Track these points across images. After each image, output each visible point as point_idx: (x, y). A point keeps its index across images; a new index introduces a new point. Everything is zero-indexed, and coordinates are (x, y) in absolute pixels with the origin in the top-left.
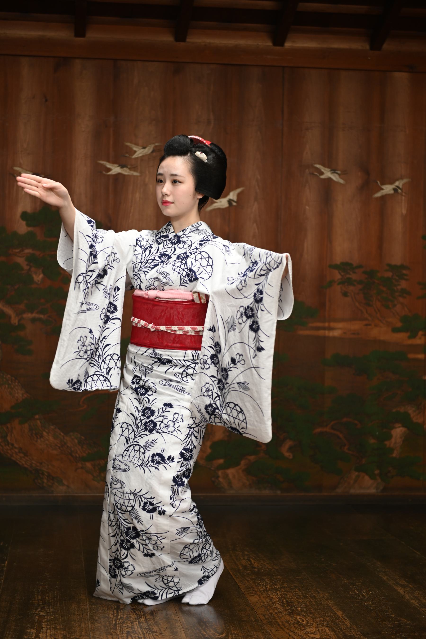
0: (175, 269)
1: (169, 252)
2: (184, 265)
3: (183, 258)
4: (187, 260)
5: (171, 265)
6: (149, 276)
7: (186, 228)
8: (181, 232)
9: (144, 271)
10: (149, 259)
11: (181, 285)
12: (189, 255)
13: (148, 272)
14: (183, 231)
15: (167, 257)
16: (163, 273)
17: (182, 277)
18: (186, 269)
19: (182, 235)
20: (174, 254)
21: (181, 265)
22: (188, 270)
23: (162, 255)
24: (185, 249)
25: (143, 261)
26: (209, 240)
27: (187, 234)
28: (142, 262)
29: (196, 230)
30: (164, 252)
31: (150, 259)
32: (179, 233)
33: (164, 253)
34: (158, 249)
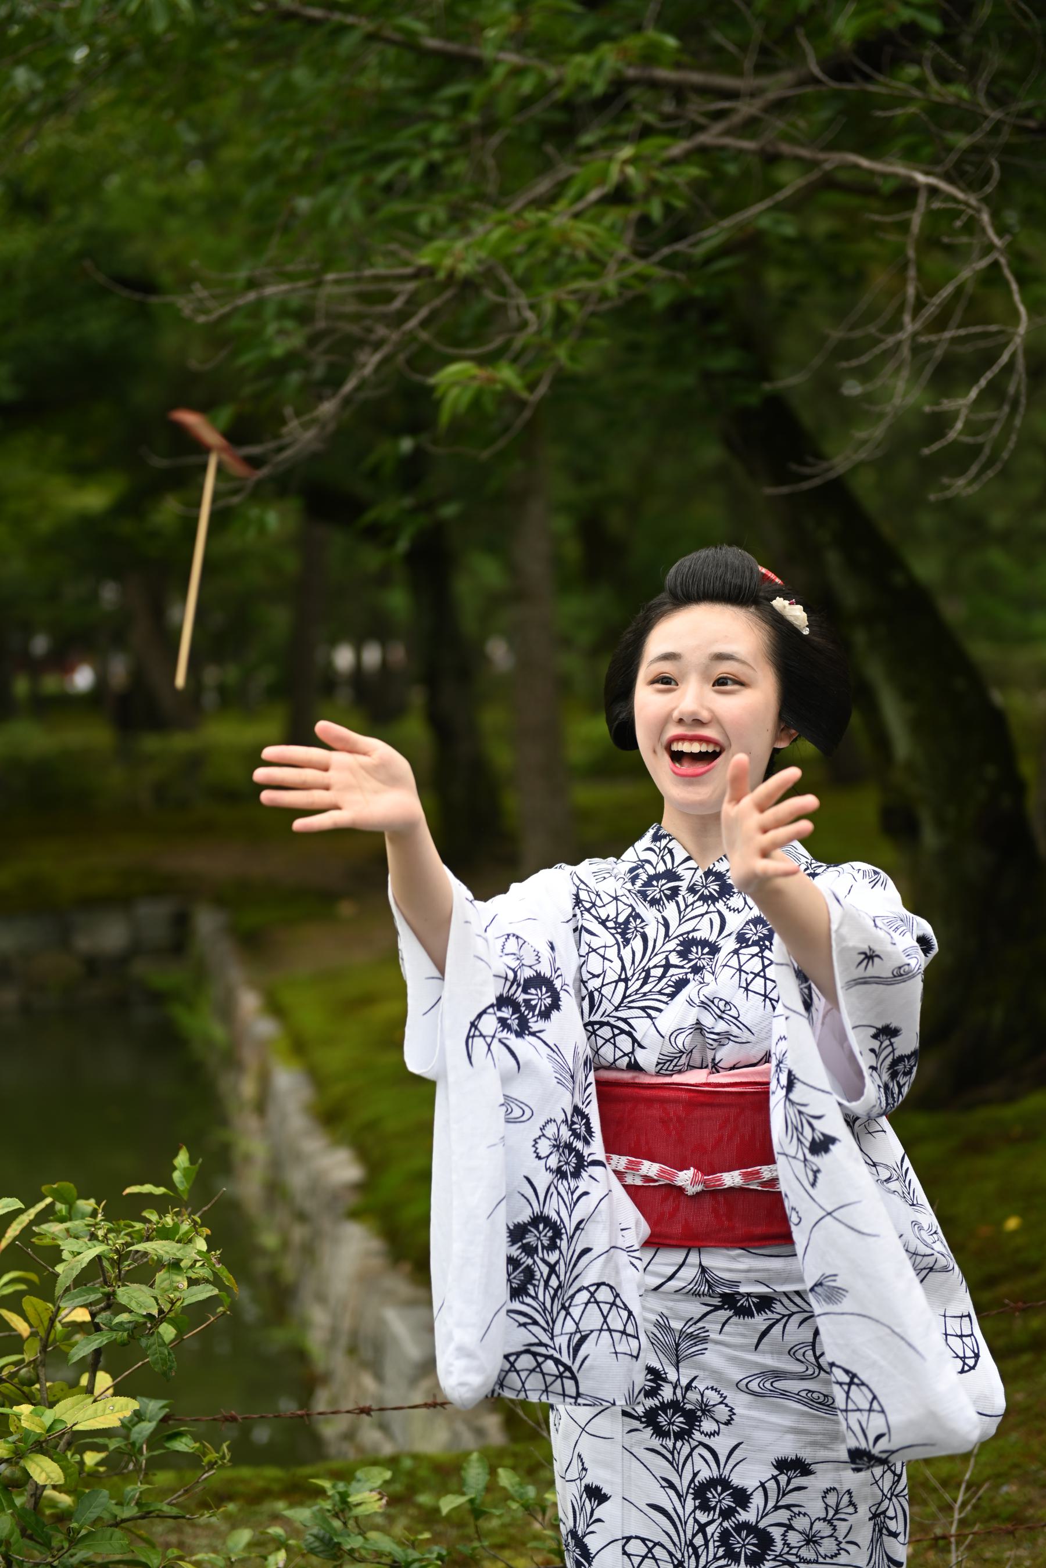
13: (660, 1010)
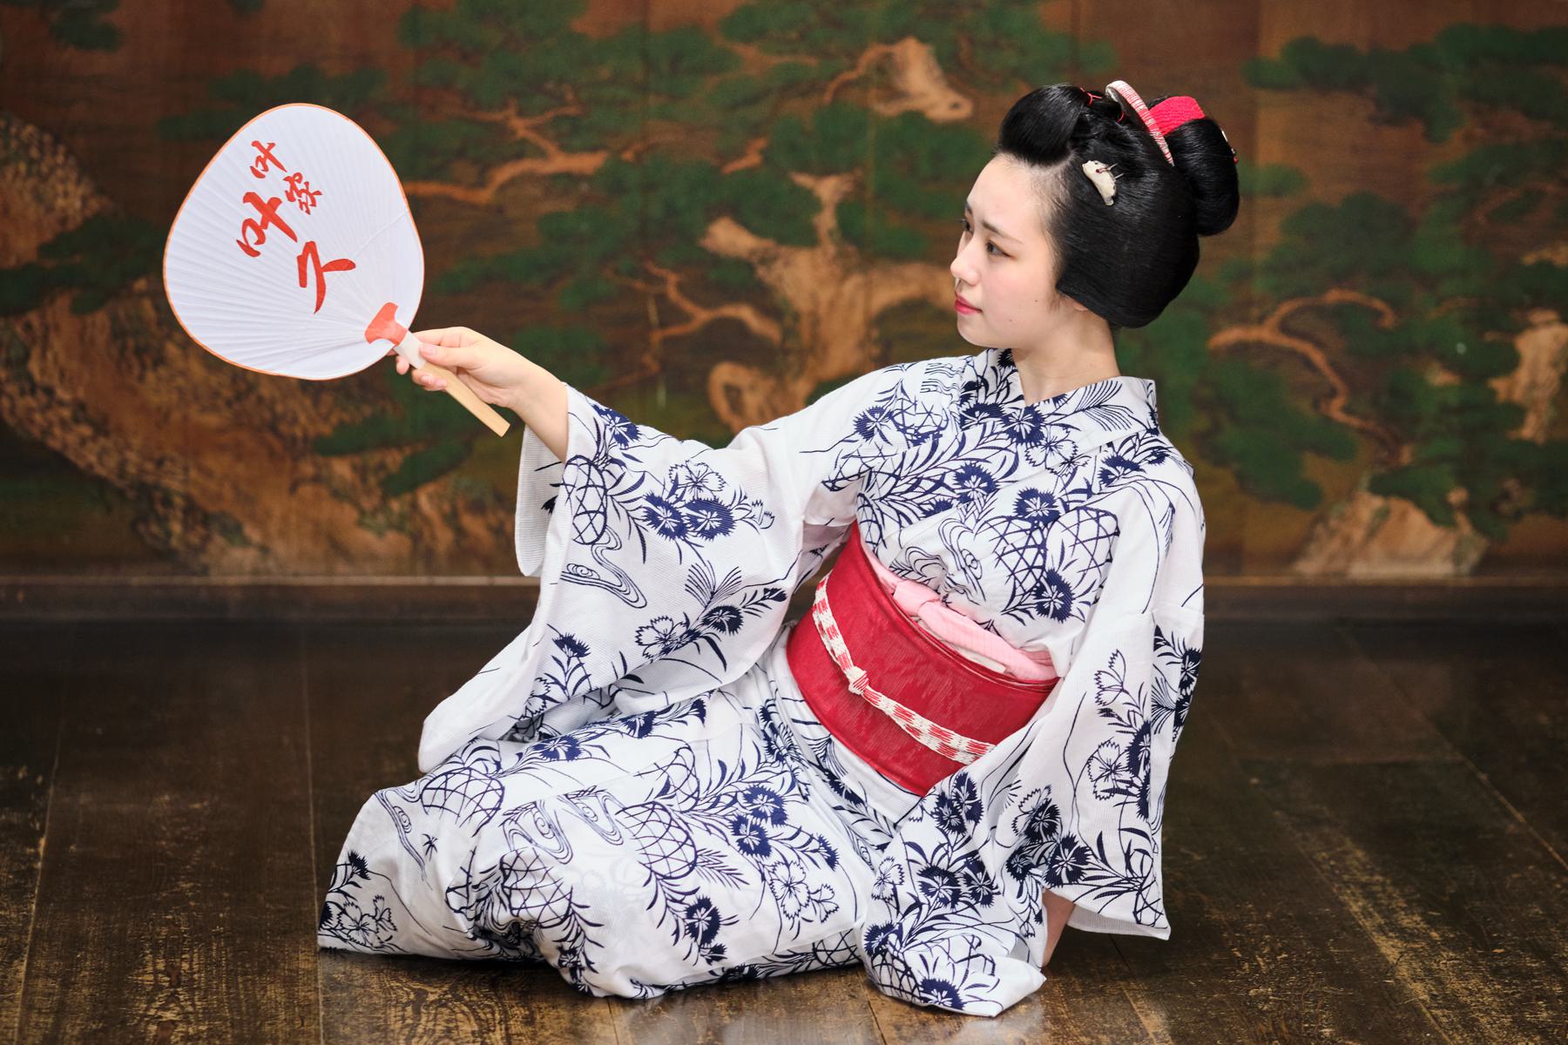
0: (1003, 554)
1: (992, 468)
2: (1035, 550)
3: (1038, 518)
4: (1049, 530)
5: (992, 533)
6: (912, 534)
7: (1069, 394)
8: (1048, 400)
9: (899, 513)
10: (926, 475)
11: (1008, 613)
12: (1058, 512)
13: (910, 522)
14: (1056, 400)
15: (985, 485)
16: (961, 552)
17: (1019, 591)
18: (1040, 571)
19: (1049, 415)
20: (1010, 478)
21: (1026, 546)
22: (1045, 574)
23: (971, 471)
24: (1049, 469)
25: (906, 477)
26: (1136, 467)
27: (1066, 416)
28: (898, 478)
29: (1099, 406)
30: (978, 460)
31: (929, 479)
32: (1042, 403)
33: (977, 465)
34: (962, 444)
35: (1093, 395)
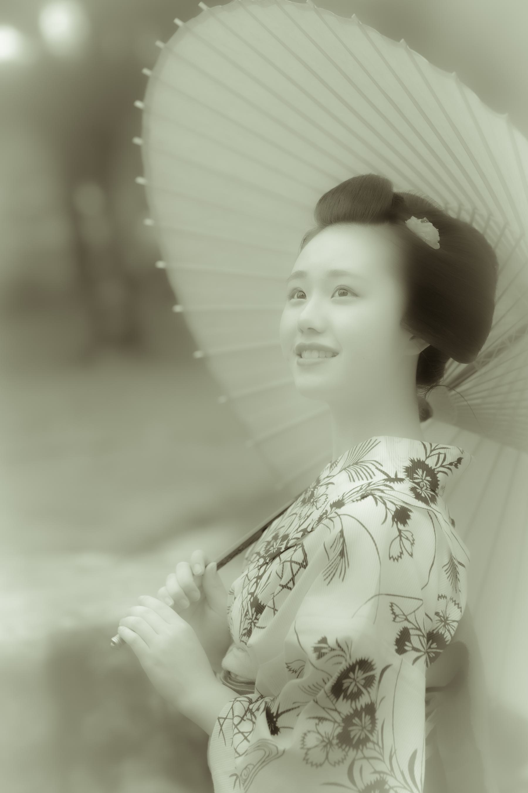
19: (324, 479)
27: (334, 476)
29: (357, 463)
35: (354, 455)
